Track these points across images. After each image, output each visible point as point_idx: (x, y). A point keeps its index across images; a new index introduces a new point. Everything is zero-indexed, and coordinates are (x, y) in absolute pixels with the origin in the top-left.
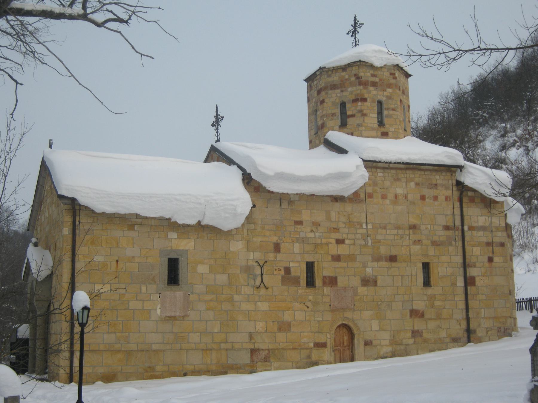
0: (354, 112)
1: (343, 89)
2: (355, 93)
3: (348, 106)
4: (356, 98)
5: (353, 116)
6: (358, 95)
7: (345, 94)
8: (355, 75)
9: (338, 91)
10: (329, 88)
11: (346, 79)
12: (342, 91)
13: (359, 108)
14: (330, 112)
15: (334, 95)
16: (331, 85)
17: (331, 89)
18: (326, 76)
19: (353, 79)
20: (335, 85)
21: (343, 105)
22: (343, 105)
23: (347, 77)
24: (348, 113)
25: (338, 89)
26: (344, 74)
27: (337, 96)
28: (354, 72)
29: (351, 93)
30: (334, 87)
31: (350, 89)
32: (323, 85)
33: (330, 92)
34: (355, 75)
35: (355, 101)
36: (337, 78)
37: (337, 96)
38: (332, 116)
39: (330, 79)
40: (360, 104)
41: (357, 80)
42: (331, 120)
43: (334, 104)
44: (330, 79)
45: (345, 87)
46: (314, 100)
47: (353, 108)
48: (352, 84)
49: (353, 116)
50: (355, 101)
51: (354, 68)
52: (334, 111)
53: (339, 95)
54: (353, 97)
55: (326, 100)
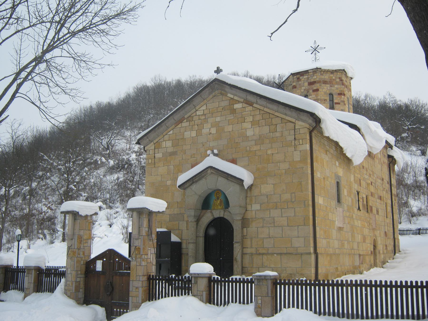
0: (339, 101)
1: (332, 85)
2: (340, 89)
3: (335, 97)
4: (340, 93)
5: (338, 103)
6: (341, 91)
7: (333, 88)
8: (339, 78)
9: (328, 86)
10: (322, 82)
11: (334, 79)
12: (331, 86)
13: (342, 99)
14: (323, 98)
15: (326, 88)
16: (323, 81)
17: (323, 83)
18: (319, 74)
19: (338, 80)
20: (326, 81)
21: (331, 95)
22: (331, 95)
23: (334, 78)
24: (335, 101)
25: (328, 84)
26: (332, 75)
27: (327, 89)
28: (338, 76)
29: (337, 88)
30: (325, 82)
31: (336, 86)
32: (318, 79)
33: (323, 85)
34: (339, 78)
35: (340, 94)
36: (328, 77)
37: (327, 89)
38: (324, 101)
39: (323, 77)
40: (343, 97)
41: (341, 82)
42: (323, 103)
43: (325, 93)
44: (323, 77)
45: (333, 84)
46: (303, 88)
47: (339, 98)
48: (337, 83)
49: (338, 103)
50: (340, 94)
51: (338, 73)
52: (325, 98)
53: (329, 88)
54: (339, 92)
55: (320, 90)
